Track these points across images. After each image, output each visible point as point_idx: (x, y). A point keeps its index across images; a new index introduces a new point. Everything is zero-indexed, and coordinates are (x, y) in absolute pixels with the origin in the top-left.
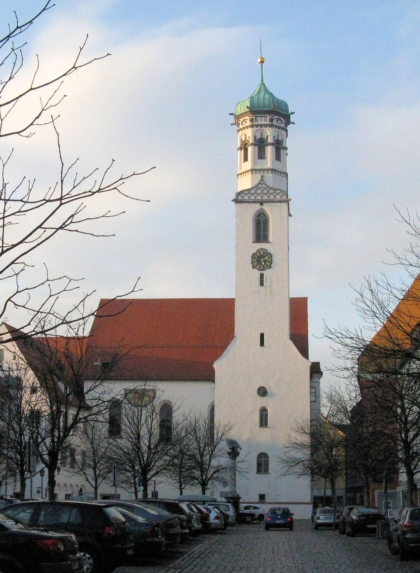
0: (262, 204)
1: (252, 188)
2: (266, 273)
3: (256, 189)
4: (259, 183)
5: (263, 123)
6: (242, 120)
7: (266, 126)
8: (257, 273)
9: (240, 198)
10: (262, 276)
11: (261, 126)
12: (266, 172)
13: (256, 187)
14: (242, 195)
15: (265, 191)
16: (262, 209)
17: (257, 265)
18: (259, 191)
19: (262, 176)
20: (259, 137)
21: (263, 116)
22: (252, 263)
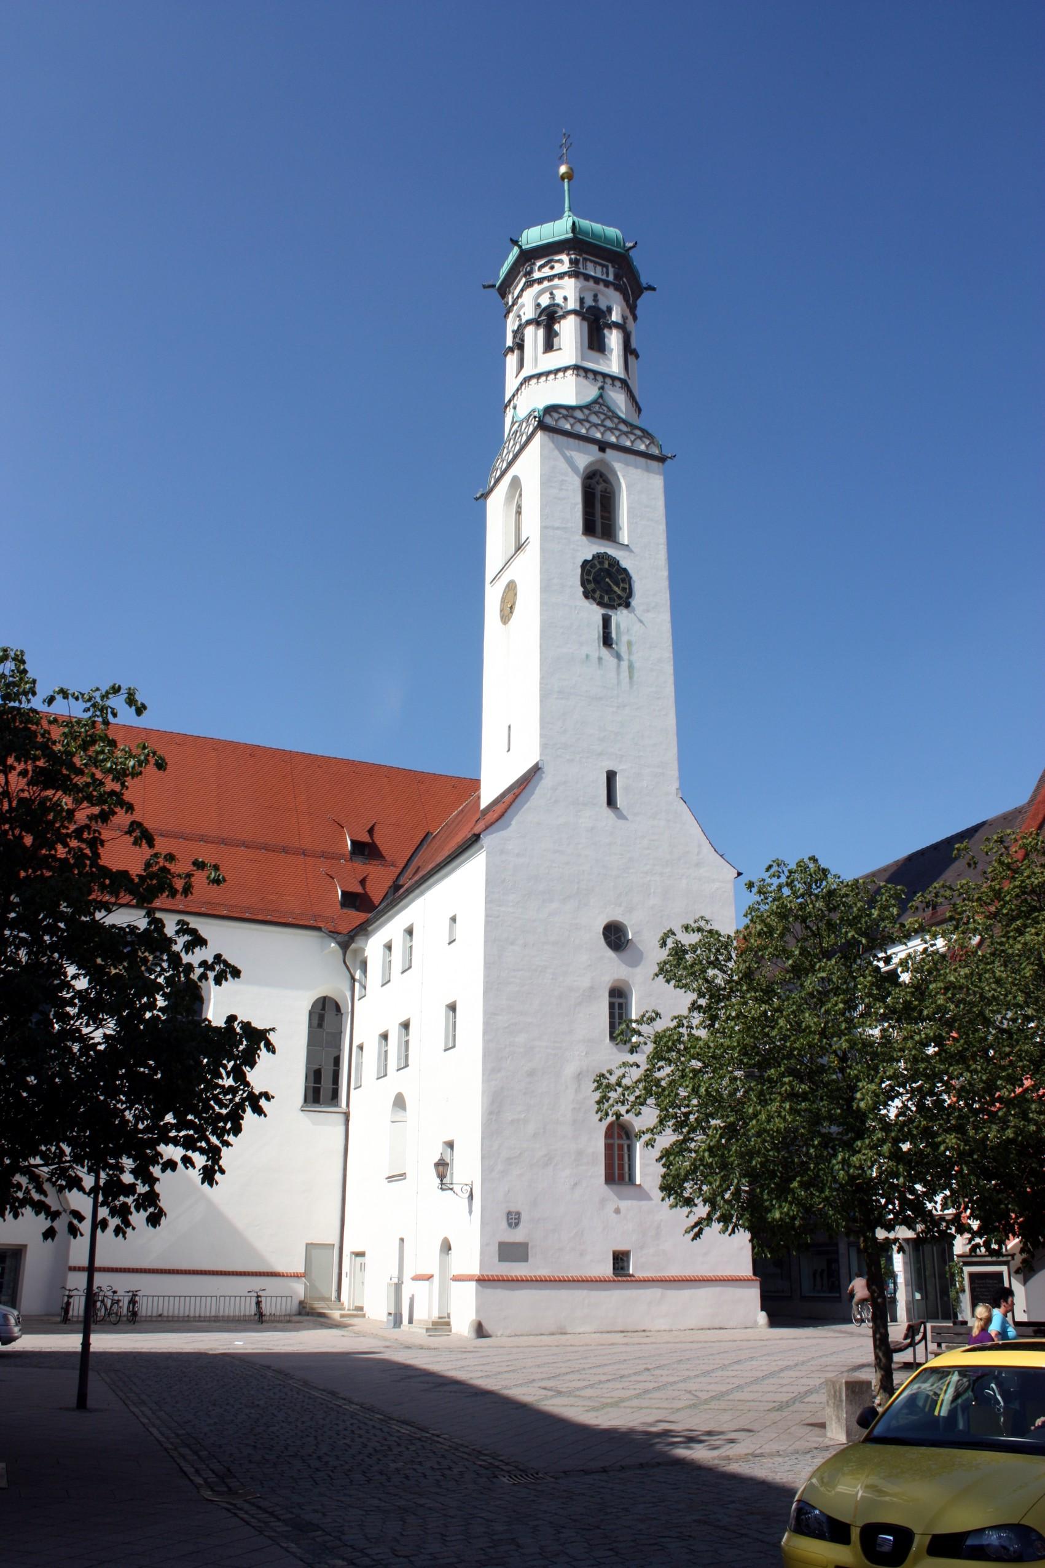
0: (602, 449)
1: (580, 408)
2: (620, 617)
3: (586, 412)
4: (595, 402)
5: (599, 275)
6: (539, 263)
7: (607, 284)
8: (594, 613)
9: (549, 420)
10: (606, 621)
11: (597, 281)
12: (609, 381)
13: (588, 407)
14: (556, 415)
15: (608, 423)
16: (602, 462)
17: (594, 591)
18: (594, 419)
19: (602, 388)
20: (589, 302)
21: (600, 264)
22: (583, 585)
